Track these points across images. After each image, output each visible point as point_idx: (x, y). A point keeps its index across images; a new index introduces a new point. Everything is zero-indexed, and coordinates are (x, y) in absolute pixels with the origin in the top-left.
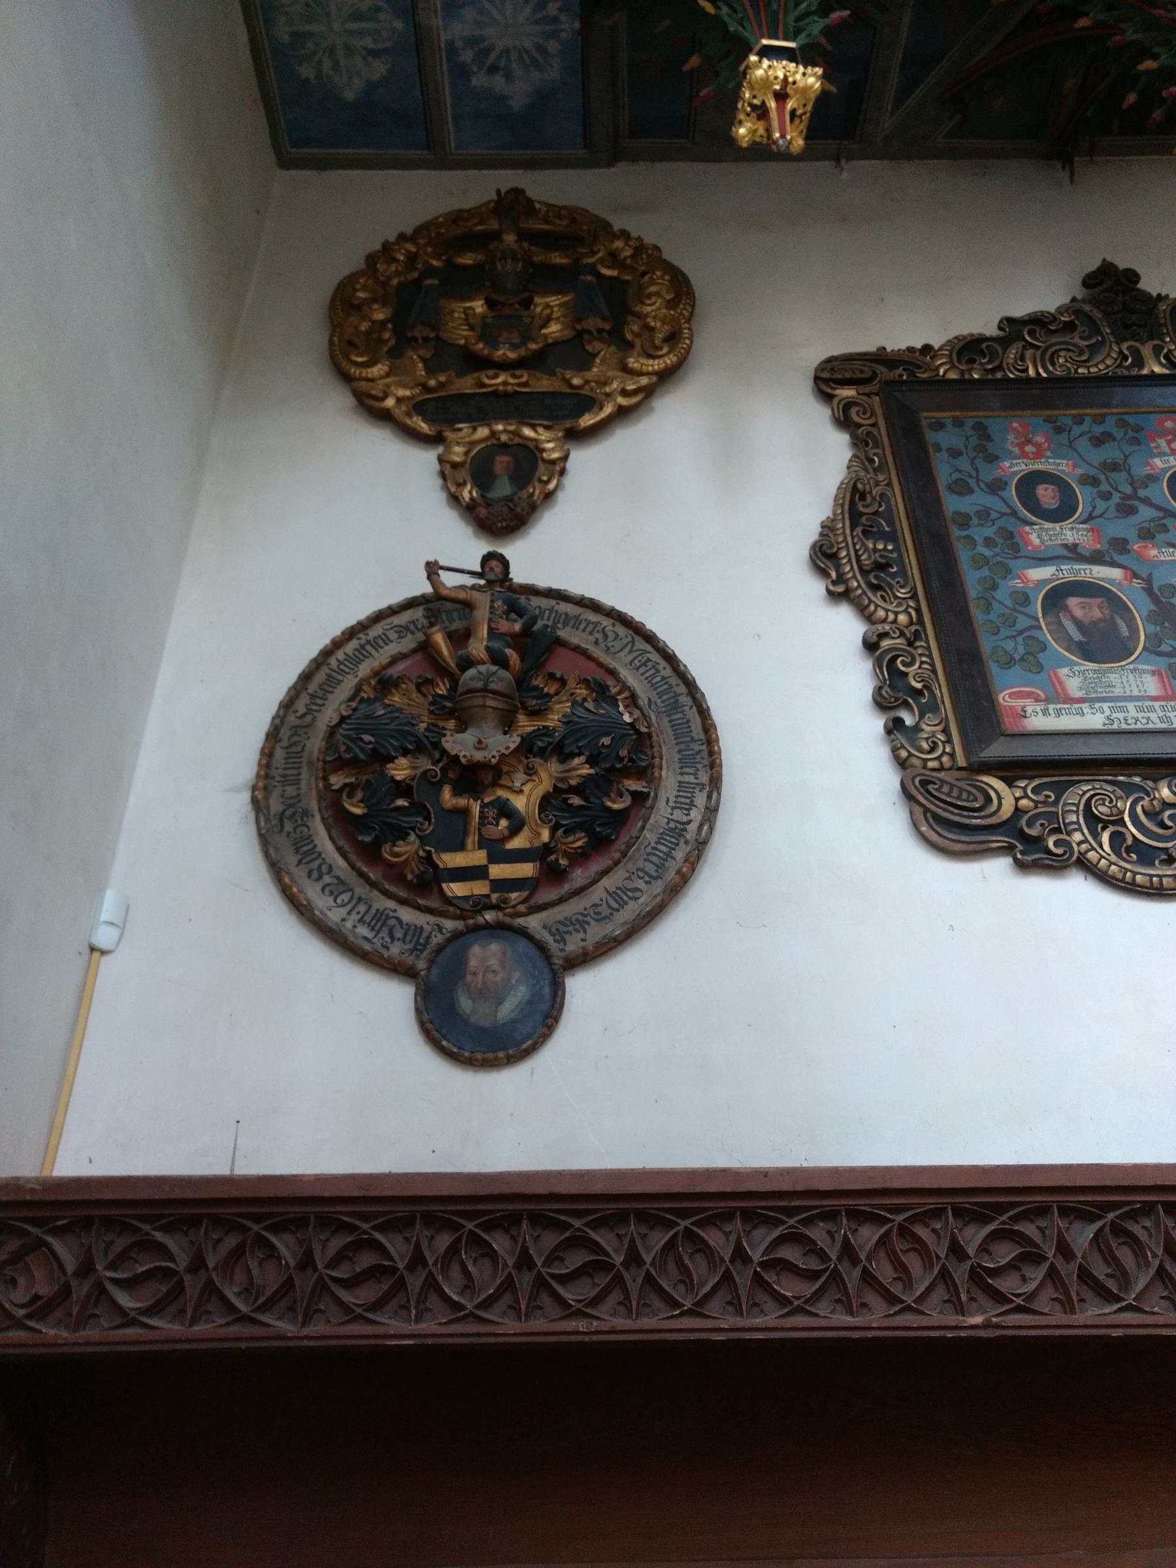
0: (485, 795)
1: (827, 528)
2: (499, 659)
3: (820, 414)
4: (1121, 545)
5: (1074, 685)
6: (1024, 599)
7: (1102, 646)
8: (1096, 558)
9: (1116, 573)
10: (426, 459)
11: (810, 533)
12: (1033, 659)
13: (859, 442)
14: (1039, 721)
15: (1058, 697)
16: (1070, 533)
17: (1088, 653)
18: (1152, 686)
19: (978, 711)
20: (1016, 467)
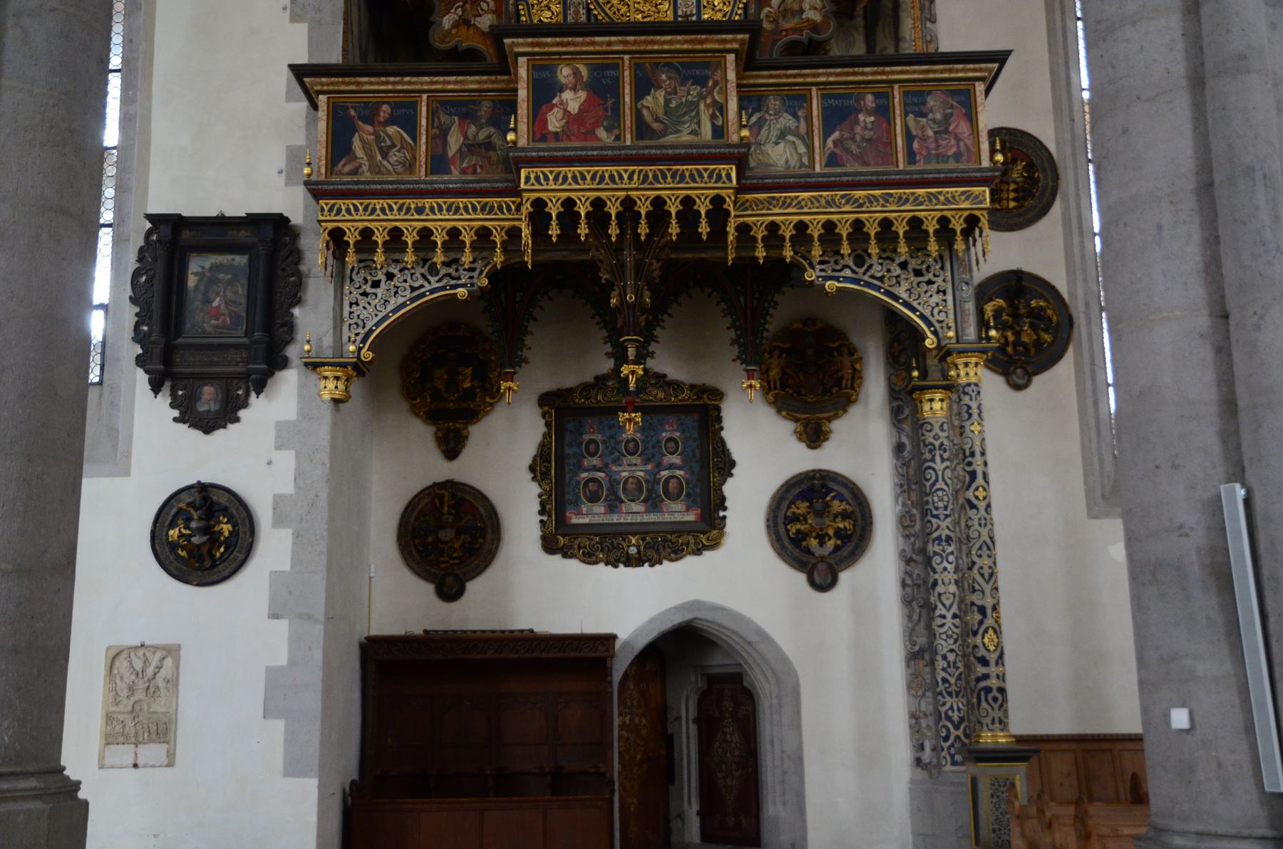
0: (449, 536)
1: (535, 459)
2: (449, 513)
3: (538, 411)
4: (607, 465)
5: (584, 510)
6: (578, 483)
7: (594, 498)
8: (600, 470)
9: (603, 475)
10: (432, 429)
11: (529, 461)
12: (577, 503)
13: (548, 425)
14: (575, 520)
15: (580, 514)
16: (595, 461)
17: (590, 500)
18: (602, 510)
19: (561, 520)
20: (587, 437)
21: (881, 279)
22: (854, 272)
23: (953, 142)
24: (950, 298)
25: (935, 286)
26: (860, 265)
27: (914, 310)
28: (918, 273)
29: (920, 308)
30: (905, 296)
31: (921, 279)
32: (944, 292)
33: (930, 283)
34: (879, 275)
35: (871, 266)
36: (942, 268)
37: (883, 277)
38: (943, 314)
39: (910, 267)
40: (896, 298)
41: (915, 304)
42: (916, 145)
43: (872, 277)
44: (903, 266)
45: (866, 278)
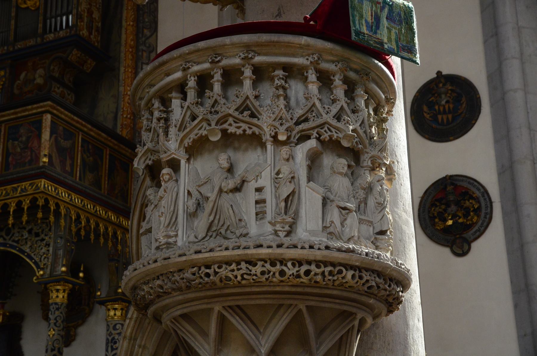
21: (17, 242)
22: (5, 239)
23: (29, 153)
24: (51, 249)
25: (45, 242)
26: (7, 234)
27: (31, 259)
28: (37, 235)
29: (35, 257)
30: (28, 250)
31: (37, 239)
32: (49, 245)
33: (43, 240)
34: (17, 239)
35: (13, 235)
36: (50, 230)
37: (19, 240)
38: (46, 259)
39: (33, 232)
40: (23, 252)
41: (32, 255)
42: (10, 159)
43: (14, 241)
44: (30, 232)
45: (10, 242)
